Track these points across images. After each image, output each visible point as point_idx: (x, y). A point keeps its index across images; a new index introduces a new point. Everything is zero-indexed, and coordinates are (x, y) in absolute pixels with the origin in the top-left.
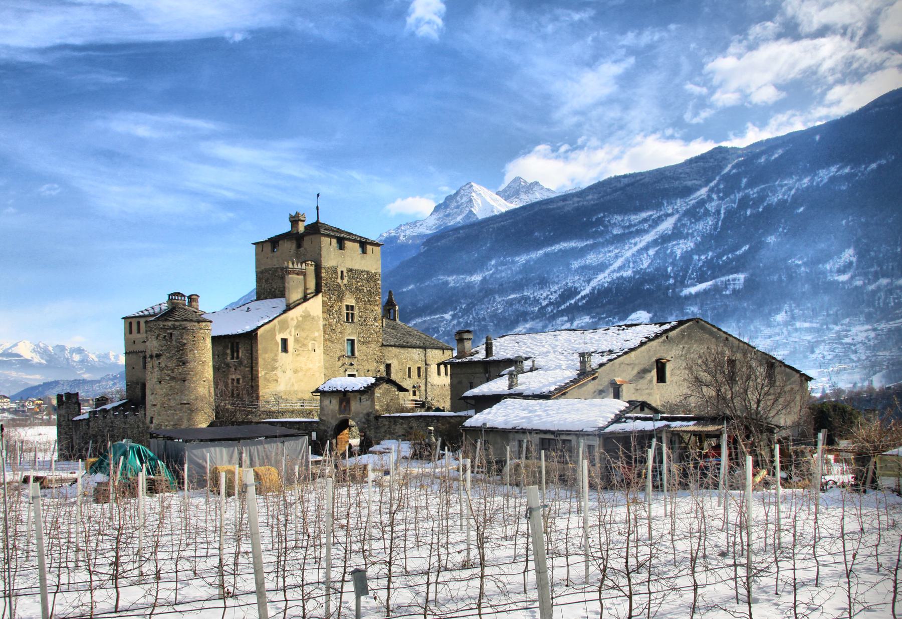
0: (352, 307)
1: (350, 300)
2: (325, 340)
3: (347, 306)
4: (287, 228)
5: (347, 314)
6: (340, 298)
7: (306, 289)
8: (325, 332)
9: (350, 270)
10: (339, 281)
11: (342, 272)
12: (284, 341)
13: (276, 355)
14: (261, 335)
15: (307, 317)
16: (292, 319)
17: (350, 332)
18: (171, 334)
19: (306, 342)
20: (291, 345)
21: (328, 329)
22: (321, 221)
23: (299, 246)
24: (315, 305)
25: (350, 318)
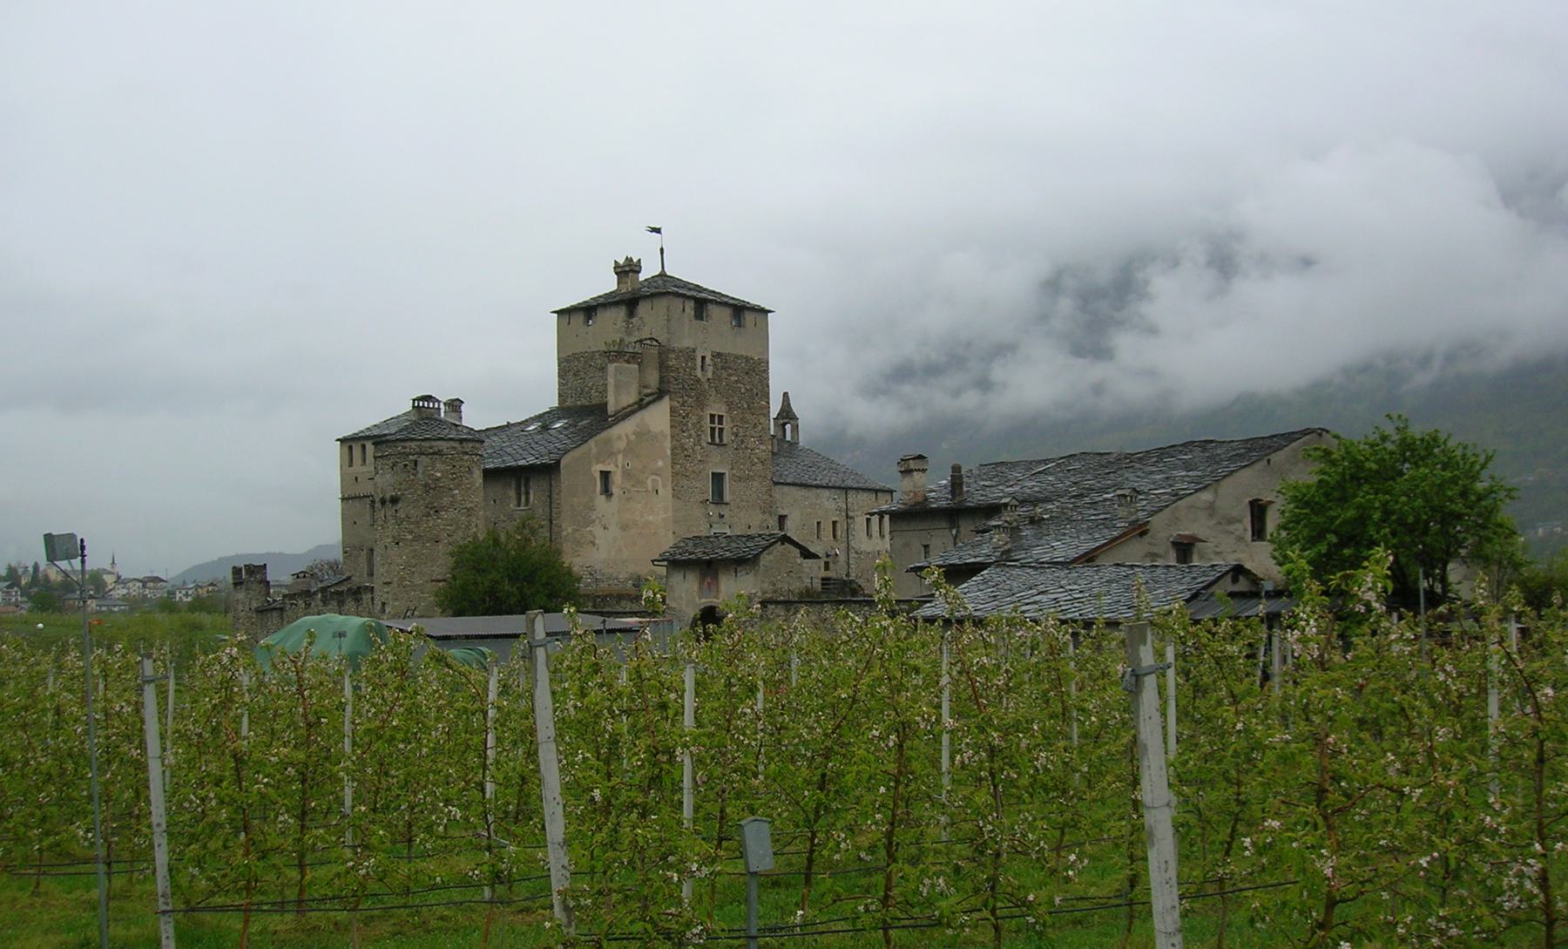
0: (721, 417)
1: (718, 408)
2: (675, 474)
3: (712, 416)
4: (609, 284)
5: (713, 429)
6: (701, 403)
9: (719, 355)
10: (699, 373)
12: (605, 475)
13: (592, 500)
15: (643, 434)
20: (617, 479)
21: (679, 451)
23: (631, 314)
24: (658, 417)
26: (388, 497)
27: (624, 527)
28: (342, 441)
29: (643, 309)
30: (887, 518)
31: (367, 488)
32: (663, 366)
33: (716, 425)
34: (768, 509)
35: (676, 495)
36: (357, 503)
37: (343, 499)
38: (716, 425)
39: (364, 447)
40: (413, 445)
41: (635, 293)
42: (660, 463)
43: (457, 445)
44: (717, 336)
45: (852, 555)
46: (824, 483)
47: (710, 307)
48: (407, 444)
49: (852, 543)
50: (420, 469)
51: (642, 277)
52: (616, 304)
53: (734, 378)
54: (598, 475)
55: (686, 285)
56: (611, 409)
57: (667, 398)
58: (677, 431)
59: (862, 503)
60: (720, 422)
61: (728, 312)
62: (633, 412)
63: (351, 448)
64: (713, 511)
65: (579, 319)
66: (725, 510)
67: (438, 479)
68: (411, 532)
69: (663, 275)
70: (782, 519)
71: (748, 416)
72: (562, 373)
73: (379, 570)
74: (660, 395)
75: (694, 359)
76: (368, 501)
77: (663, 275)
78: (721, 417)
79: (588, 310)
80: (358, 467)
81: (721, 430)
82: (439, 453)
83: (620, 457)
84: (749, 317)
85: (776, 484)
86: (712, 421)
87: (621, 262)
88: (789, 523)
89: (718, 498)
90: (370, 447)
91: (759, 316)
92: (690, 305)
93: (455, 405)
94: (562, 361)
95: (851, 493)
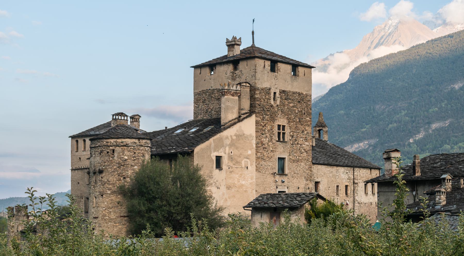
0: (284, 127)
1: (282, 121)
2: (258, 158)
3: (279, 126)
4: (223, 51)
5: (279, 133)
6: (273, 119)
7: (240, 109)
8: (257, 152)
9: (284, 92)
10: (272, 102)
11: (275, 93)
12: (219, 159)
13: (211, 172)
14: (197, 153)
15: (240, 136)
16: (227, 138)
17: (281, 151)
18: (113, 151)
19: (239, 160)
20: (225, 162)
21: (260, 145)
22: (257, 45)
23: (235, 68)
24: (249, 126)
25: (281, 138)
26: (97, 169)
27: (229, 188)
28: (73, 137)
29: (242, 65)
30: (376, 185)
31: (86, 164)
32: (252, 98)
33: (281, 131)
34: (309, 178)
35: (258, 170)
36: (80, 172)
37: (72, 170)
38: (281, 131)
39: (84, 141)
40: (112, 141)
41: (238, 58)
42: (249, 152)
43: (137, 141)
44: (282, 81)
45: (356, 204)
46: (341, 164)
47: (280, 65)
48: (109, 140)
49: (356, 198)
50: (116, 154)
51: (242, 48)
52: (227, 63)
53: (291, 105)
54: (214, 159)
55: (266, 52)
56: (223, 122)
57: (254, 117)
58: (259, 134)
59: (363, 174)
60: (284, 129)
61: (289, 67)
62: (235, 124)
63: (77, 141)
64: (278, 178)
65: (207, 70)
66: (285, 179)
67: (126, 160)
68: (109, 189)
69: (253, 46)
70: (317, 183)
71: (299, 126)
72: (196, 101)
73: (92, 210)
74: (251, 113)
75: (269, 94)
76: (86, 171)
77: (253, 46)
78: (284, 127)
79: (212, 65)
80: (81, 153)
81: (284, 134)
82: (126, 145)
83: (227, 148)
84: (300, 69)
85: (314, 164)
86: (279, 129)
87: (230, 39)
88: (321, 187)
89: (282, 171)
90: (87, 140)
91: (306, 70)
92: (268, 63)
93: (135, 118)
94: (195, 94)
95: (356, 169)
